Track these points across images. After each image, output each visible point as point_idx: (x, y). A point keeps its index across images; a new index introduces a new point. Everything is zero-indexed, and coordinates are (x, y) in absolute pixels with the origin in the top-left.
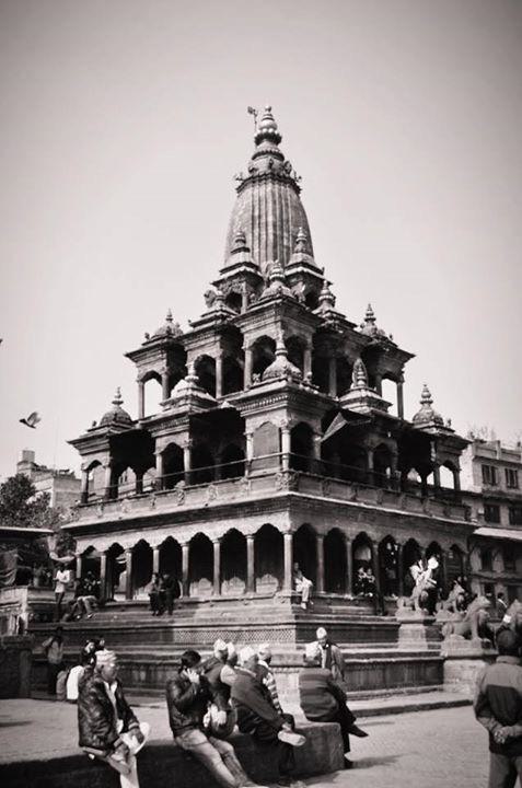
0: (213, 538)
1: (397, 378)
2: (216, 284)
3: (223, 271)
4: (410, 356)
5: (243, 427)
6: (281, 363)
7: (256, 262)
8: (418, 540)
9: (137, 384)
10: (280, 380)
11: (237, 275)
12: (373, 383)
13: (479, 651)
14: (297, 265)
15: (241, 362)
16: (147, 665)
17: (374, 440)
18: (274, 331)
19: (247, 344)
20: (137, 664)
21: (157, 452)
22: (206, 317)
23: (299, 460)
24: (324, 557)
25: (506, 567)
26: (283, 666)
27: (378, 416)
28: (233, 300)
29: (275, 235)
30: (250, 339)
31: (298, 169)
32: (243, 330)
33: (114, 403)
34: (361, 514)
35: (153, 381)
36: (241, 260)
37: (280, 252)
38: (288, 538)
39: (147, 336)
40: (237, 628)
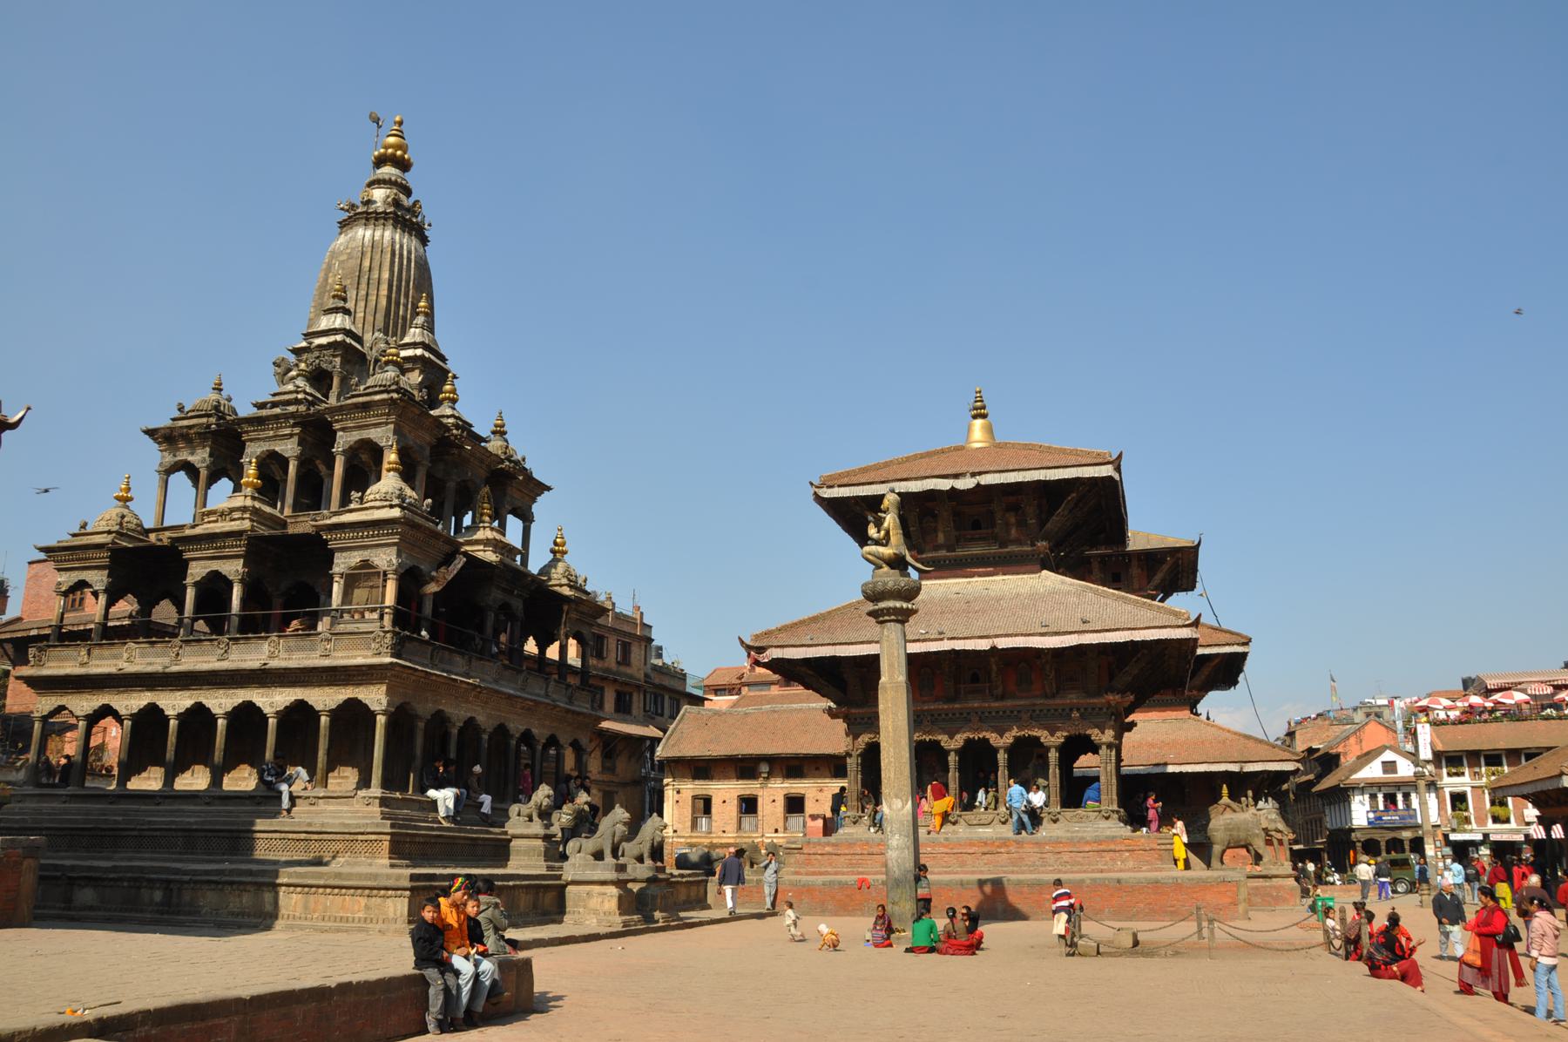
0: (267, 710)
1: (527, 518)
2: (297, 352)
3: (308, 336)
4: (543, 488)
5: (330, 563)
6: (389, 482)
7: (358, 332)
8: (535, 731)
9: (157, 476)
10: (391, 507)
11: (330, 345)
12: (498, 515)
13: (612, 875)
14: (414, 345)
15: (322, 468)
16: (169, 882)
17: (495, 596)
18: (383, 435)
19: (338, 448)
20: (150, 880)
21: (189, 580)
22: (277, 398)
23: (406, 615)
24: (419, 749)
25: (603, 767)
26: (325, 887)
27: (505, 565)
28: (320, 378)
29: (389, 298)
30: (343, 441)
31: (429, 214)
32: (337, 426)
33: (118, 498)
34: (470, 695)
35: (181, 475)
36: (337, 325)
37: (394, 325)
38: (381, 720)
39: (181, 409)
40: (303, 836)
